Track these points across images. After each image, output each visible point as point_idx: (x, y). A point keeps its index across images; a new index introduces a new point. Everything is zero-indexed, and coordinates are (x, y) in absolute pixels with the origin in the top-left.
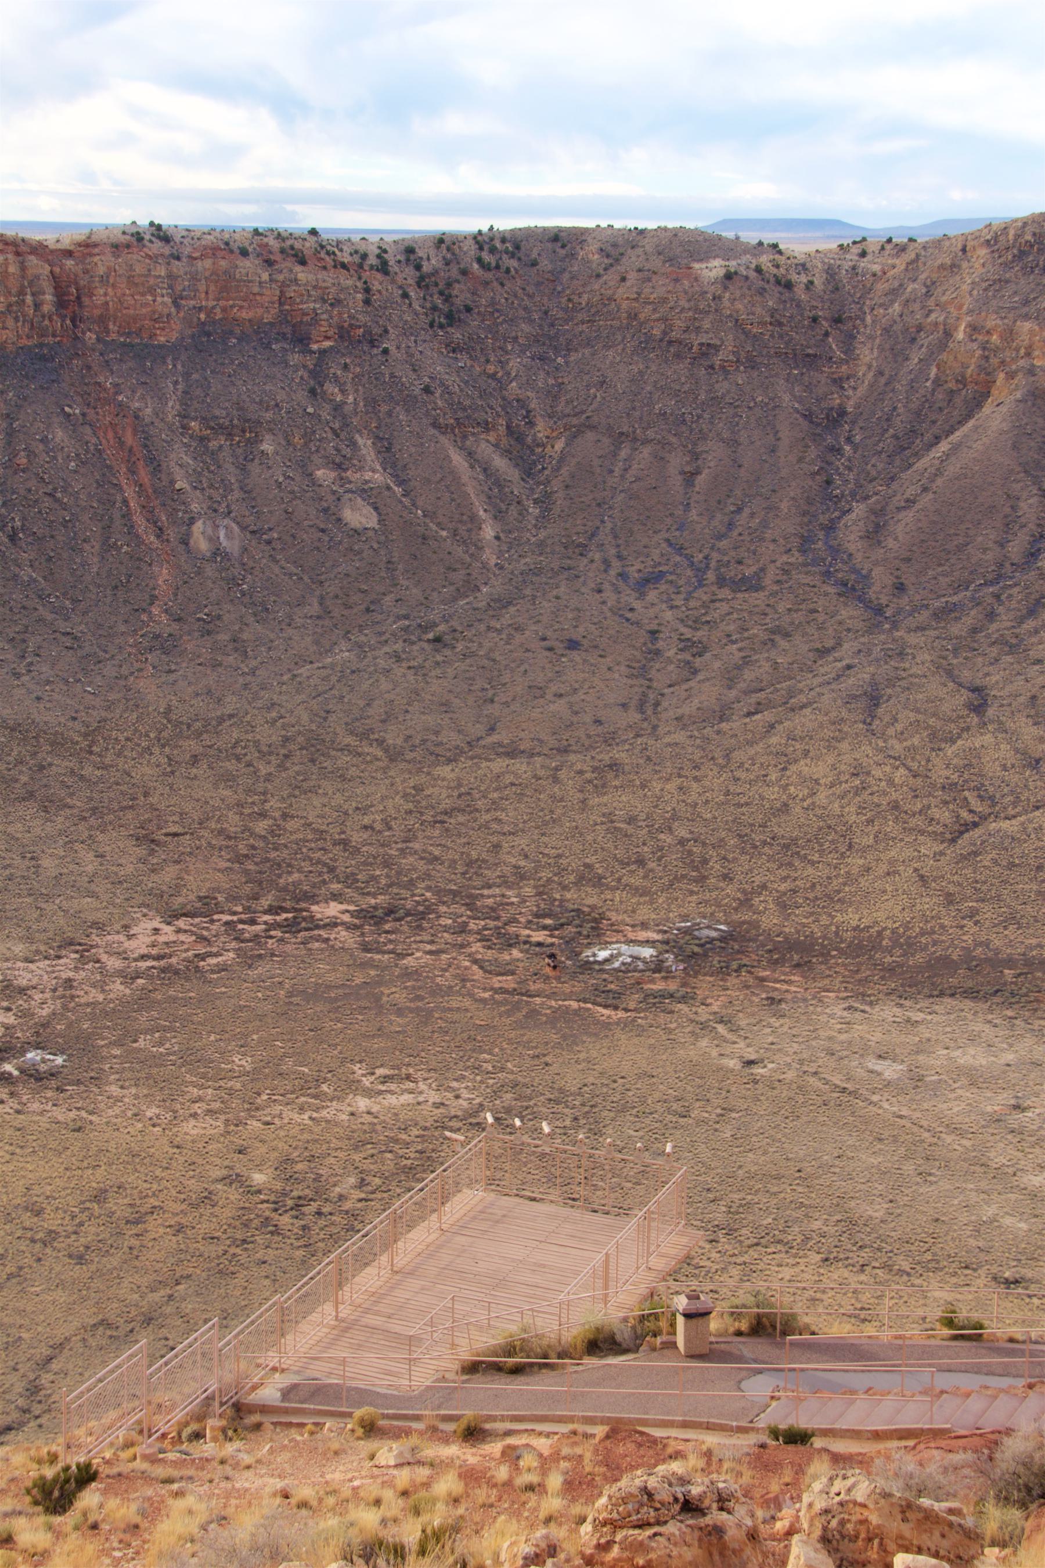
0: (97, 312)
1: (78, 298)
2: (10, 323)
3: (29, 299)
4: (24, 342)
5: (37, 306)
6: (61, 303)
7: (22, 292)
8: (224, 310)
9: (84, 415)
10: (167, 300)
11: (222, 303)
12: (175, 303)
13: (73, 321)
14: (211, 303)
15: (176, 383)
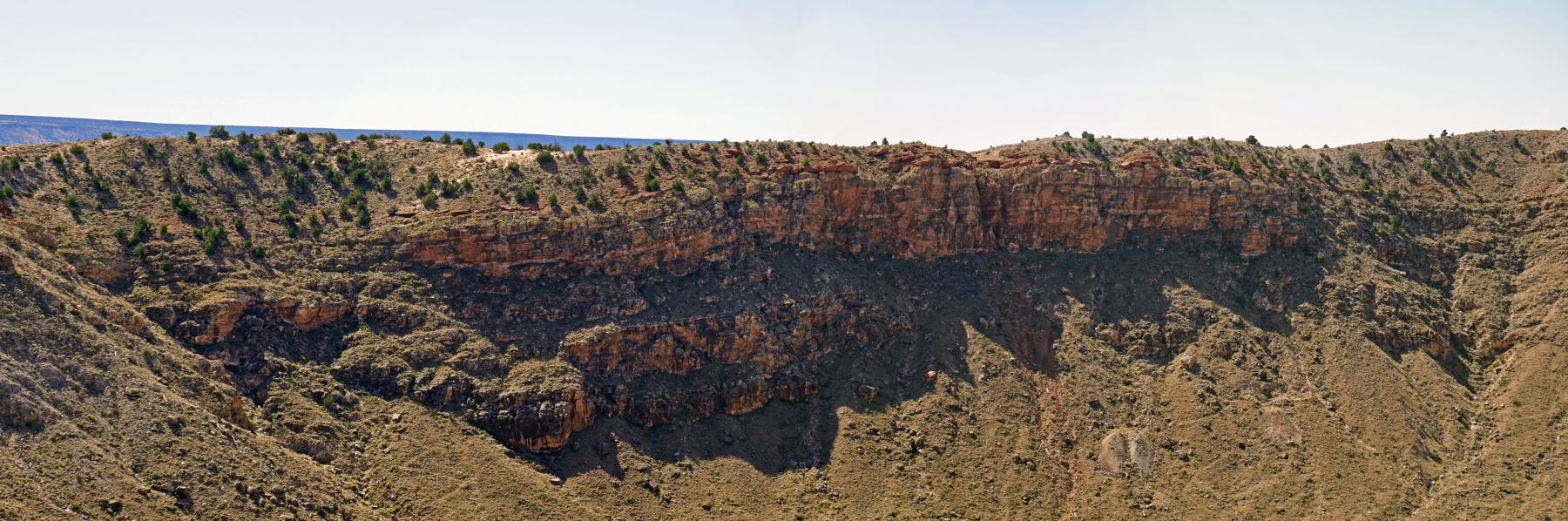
0: (1021, 221)
1: (1003, 208)
2: (931, 232)
3: (952, 211)
4: (945, 252)
5: (960, 218)
6: (985, 215)
7: (944, 204)
8: (1152, 218)
9: (999, 325)
10: (1094, 209)
11: (1151, 211)
12: (1103, 213)
13: (996, 232)
14: (1139, 212)
15: (1099, 292)
